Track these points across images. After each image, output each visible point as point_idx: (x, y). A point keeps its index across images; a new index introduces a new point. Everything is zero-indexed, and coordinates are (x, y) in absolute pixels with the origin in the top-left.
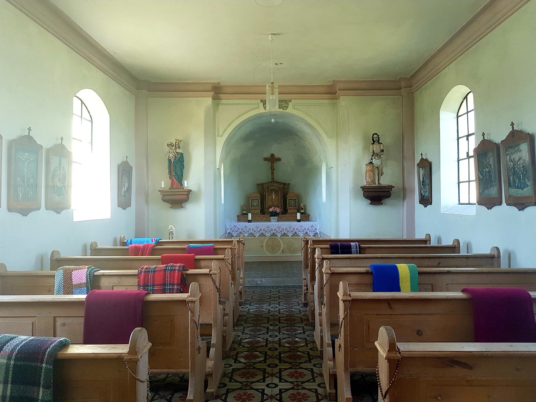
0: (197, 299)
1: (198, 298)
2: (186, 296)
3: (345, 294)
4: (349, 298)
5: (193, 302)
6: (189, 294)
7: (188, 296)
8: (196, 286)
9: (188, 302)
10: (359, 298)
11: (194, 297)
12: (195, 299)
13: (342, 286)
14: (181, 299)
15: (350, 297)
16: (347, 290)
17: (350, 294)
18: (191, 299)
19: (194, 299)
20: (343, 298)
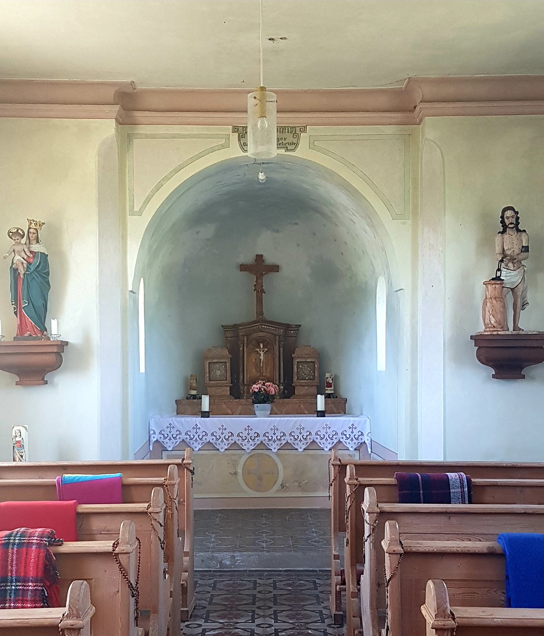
0: (84, 622)
1: (88, 618)
2: (59, 616)
3: (441, 613)
4: (451, 623)
5: (74, 629)
6: (66, 610)
7: (63, 615)
8: (82, 591)
9: (63, 630)
10: (475, 622)
11: (78, 617)
12: (81, 622)
13: (433, 592)
14: (46, 622)
15: (454, 619)
16: (446, 602)
17: (451, 612)
18: (70, 622)
19: (78, 623)
20: (436, 623)
